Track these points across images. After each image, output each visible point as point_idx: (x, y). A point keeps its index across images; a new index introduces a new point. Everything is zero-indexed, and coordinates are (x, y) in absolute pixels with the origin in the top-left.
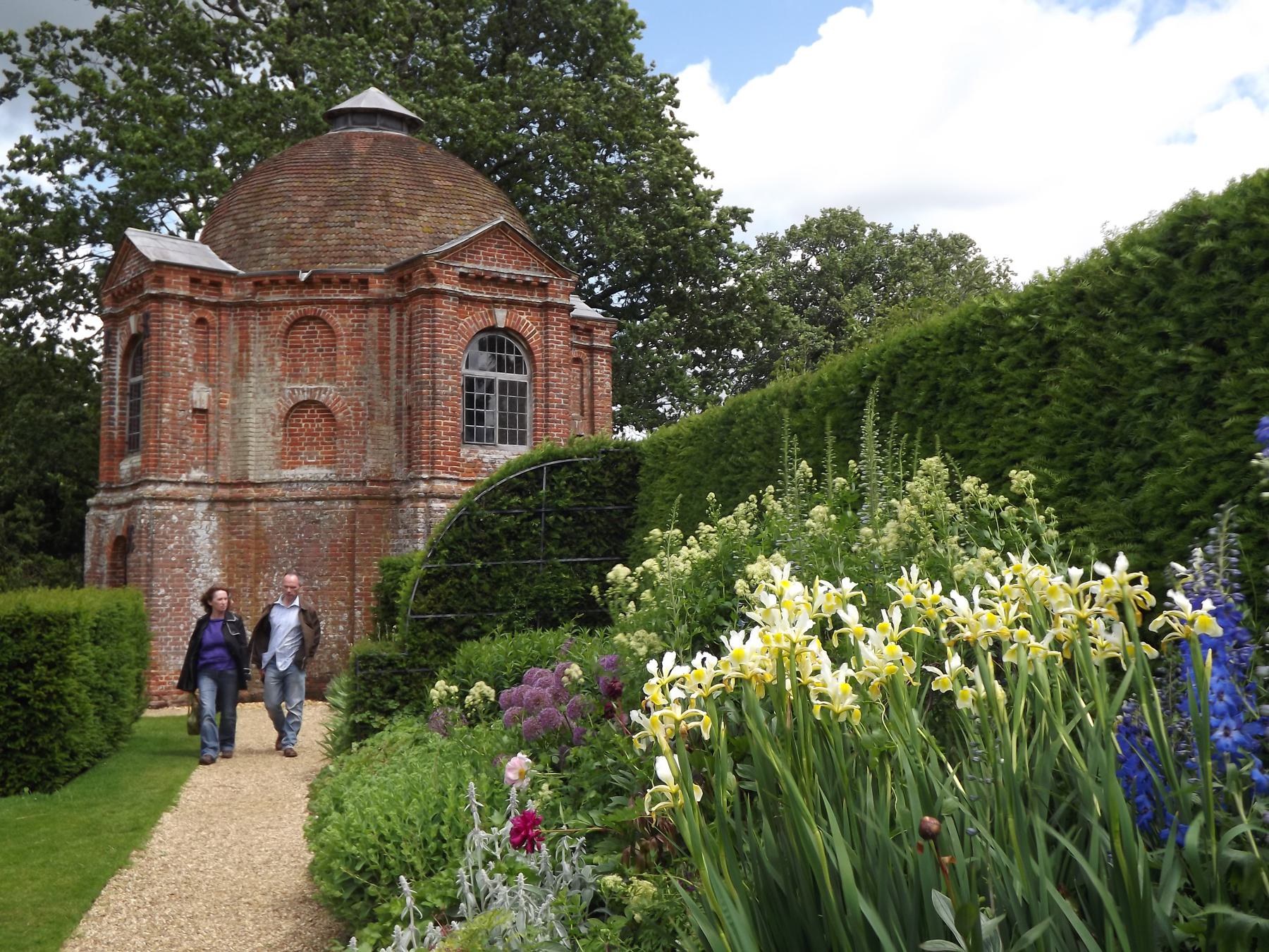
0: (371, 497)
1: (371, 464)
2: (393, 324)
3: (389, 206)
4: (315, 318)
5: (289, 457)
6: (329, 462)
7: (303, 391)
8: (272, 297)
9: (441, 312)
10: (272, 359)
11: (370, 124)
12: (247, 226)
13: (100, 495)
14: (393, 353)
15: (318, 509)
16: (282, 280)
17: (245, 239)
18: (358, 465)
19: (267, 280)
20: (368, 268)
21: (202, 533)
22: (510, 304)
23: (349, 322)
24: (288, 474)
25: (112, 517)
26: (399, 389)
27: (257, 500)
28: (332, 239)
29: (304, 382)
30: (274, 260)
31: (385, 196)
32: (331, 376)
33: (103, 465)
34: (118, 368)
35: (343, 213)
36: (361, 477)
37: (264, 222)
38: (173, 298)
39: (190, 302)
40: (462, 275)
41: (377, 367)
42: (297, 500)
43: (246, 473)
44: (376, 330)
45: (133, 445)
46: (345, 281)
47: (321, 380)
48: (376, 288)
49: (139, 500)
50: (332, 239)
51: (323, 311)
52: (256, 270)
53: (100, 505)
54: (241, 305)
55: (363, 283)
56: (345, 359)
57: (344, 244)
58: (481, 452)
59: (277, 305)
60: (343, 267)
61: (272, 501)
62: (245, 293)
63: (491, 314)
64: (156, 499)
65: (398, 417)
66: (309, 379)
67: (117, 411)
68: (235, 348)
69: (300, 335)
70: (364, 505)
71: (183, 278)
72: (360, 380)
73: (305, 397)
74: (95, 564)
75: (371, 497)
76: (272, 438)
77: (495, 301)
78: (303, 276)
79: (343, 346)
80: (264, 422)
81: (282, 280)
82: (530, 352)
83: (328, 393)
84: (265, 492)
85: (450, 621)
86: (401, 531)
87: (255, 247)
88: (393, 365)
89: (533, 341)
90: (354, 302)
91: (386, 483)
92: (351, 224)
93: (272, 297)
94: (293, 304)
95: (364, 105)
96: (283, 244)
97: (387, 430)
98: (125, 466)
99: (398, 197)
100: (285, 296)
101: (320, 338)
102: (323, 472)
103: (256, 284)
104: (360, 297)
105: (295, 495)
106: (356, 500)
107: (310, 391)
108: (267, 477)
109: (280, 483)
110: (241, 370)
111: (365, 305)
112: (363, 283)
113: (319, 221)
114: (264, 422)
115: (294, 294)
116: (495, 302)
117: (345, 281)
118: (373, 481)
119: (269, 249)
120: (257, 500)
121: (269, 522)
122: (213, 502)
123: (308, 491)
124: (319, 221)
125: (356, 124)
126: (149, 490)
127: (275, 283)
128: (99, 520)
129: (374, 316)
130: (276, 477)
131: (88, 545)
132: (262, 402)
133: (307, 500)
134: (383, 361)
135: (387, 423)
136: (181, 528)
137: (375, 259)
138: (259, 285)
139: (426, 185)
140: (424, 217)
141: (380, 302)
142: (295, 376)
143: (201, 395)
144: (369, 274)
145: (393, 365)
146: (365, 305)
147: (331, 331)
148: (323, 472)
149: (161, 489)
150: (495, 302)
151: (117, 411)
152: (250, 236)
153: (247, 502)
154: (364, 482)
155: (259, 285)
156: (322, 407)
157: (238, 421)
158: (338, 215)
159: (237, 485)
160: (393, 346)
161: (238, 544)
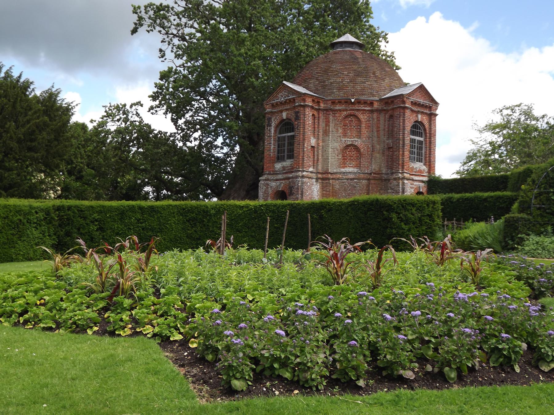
0: (374, 179)
1: (374, 167)
3: (376, 77)
6: (356, 166)
7: (349, 141)
9: (407, 115)
10: (337, 129)
11: (351, 47)
12: (324, 82)
15: (355, 182)
16: (343, 101)
17: (324, 87)
19: (337, 101)
20: (372, 98)
21: (315, 189)
23: (366, 117)
24: (343, 170)
25: (273, 184)
27: (332, 179)
29: (348, 138)
30: (338, 95)
31: (374, 73)
32: (359, 136)
34: (273, 131)
35: (361, 79)
36: (369, 172)
37: (332, 81)
38: (308, 106)
39: (312, 107)
40: (412, 102)
41: (376, 133)
42: (348, 179)
43: (328, 169)
44: (376, 120)
47: (354, 137)
48: (376, 105)
49: (297, 177)
51: (357, 113)
52: (329, 98)
54: (326, 110)
55: (371, 104)
56: (364, 130)
57: (363, 89)
59: (340, 110)
60: (363, 98)
61: (338, 179)
62: (329, 105)
63: (417, 116)
64: (303, 177)
65: (384, 151)
66: (350, 137)
67: (272, 146)
68: (324, 125)
71: (310, 100)
72: (369, 138)
73: (350, 143)
75: (374, 179)
76: (337, 157)
77: (419, 112)
78: (353, 100)
79: (363, 125)
80: (334, 151)
81: (343, 101)
82: (425, 130)
83: (358, 142)
84: (334, 176)
85: (544, 208)
86: (390, 191)
87: (329, 89)
88: (382, 133)
89: (427, 126)
90: (368, 110)
91: (378, 174)
93: (337, 108)
94: (346, 110)
96: (340, 89)
98: (278, 166)
99: (378, 73)
100: (342, 107)
102: (355, 170)
103: (332, 102)
104: (369, 109)
105: (347, 177)
106: (369, 179)
107: (352, 141)
108: (335, 171)
109: (340, 173)
110: (326, 133)
111: (372, 111)
112: (371, 104)
114: (334, 151)
115: (346, 106)
116: (418, 112)
118: (374, 173)
119: (335, 90)
120: (332, 179)
121: (337, 187)
122: (317, 179)
123: (352, 176)
125: (346, 47)
126: (300, 174)
127: (340, 102)
129: (375, 115)
130: (339, 171)
132: (335, 144)
133: (351, 179)
134: (378, 131)
135: (379, 153)
136: (310, 188)
137: (374, 96)
138: (333, 103)
140: (386, 81)
141: (377, 110)
142: (345, 135)
143: (313, 142)
144: (374, 100)
145: (382, 133)
146: (372, 111)
147: (359, 120)
148: (355, 170)
149: (304, 173)
150: (418, 112)
151: (272, 146)
152: (326, 85)
153: (329, 179)
154: (371, 174)
155: (333, 103)
157: (325, 151)
158: (360, 79)
159: (324, 173)
161: (326, 194)
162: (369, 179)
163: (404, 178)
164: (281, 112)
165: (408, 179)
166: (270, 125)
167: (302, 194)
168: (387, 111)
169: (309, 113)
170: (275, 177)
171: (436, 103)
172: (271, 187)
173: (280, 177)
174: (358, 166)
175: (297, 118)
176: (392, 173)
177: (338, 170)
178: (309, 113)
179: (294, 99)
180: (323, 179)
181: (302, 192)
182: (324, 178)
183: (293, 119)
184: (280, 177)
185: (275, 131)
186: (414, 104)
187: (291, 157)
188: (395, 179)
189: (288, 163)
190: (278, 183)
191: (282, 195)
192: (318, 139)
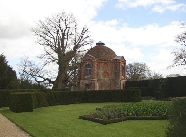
4: (107, 64)
5: (104, 77)
24: (104, 78)
25: (85, 82)
46: (109, 61)
51: (108, 64)
62: (100, 61)
64: (95, 80)
88: (114, 68)
94: (104, 62)
98: (86, 77)
101: (107, 66)
102: (107, 78)
108: (102, 79)
110: (99, 68)
112: (111, 61)
113: (106, 55)
117: (109, 61)
124: (106, 55)
127: (103, 60)
132: (101, 72)
136: (96, 83)
142: (104, 69)
155: (101, 60)
156: (107, 73)
162: (111, 81)
163: (120, 80)
164: (87, 62)
165: (121, 81)
167: (95, 85)
168: (115, 63)
169: (95, 63)
170: (86, 80)
171: (126, 61)
172: (84, 83)
173: (87, 80)
174: (108, 77)
175: (92, 64)
176: (117, 79)
178: (95, 63)
179: (91, 59)
180: (99, 81)
181: (95, 84)
182: (99, 80)
183: (91, 65)
184: (87, 80)
185: (85, 68)
186: (122, 61)
187: (90, 74)
188: (118, 81)
189: (89, 76)
190: (87, 82)
191: (88, 85)
192: (97, 70)
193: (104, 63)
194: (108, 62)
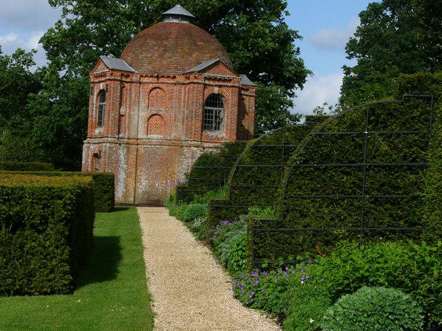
2: (183, 91)
4: (159, 88)
6: (161, 133)
8: (146, 80)
13: (88, 139)
14: (182, 100)
18: (170, 135)
22: (220, 86)
25: (92, 147)
26: (184, 112)
28: (165, 62)
33: (89, 130)
45: (100, 124)
50: (165, 62)
53: (89, 143)
58: (209, 133)
69: (154, 92)
70: (172, 147)
73: (155, 112)
74: (87, 162)
83: (163, 111)
92: (171, 58)
95: (173, 13)
96: (150, 63)
97: (180, 124)
98: (97, 131)
124: (161, 56)
128: (89, 147)
129: (176, 88)
131: (83, 156)
139: (195, 44)
160: (182, 98)
166: (92, 94)
177: (145, 136)
185: (97, 99)
193: (151, 86)
194: (166, 80)
